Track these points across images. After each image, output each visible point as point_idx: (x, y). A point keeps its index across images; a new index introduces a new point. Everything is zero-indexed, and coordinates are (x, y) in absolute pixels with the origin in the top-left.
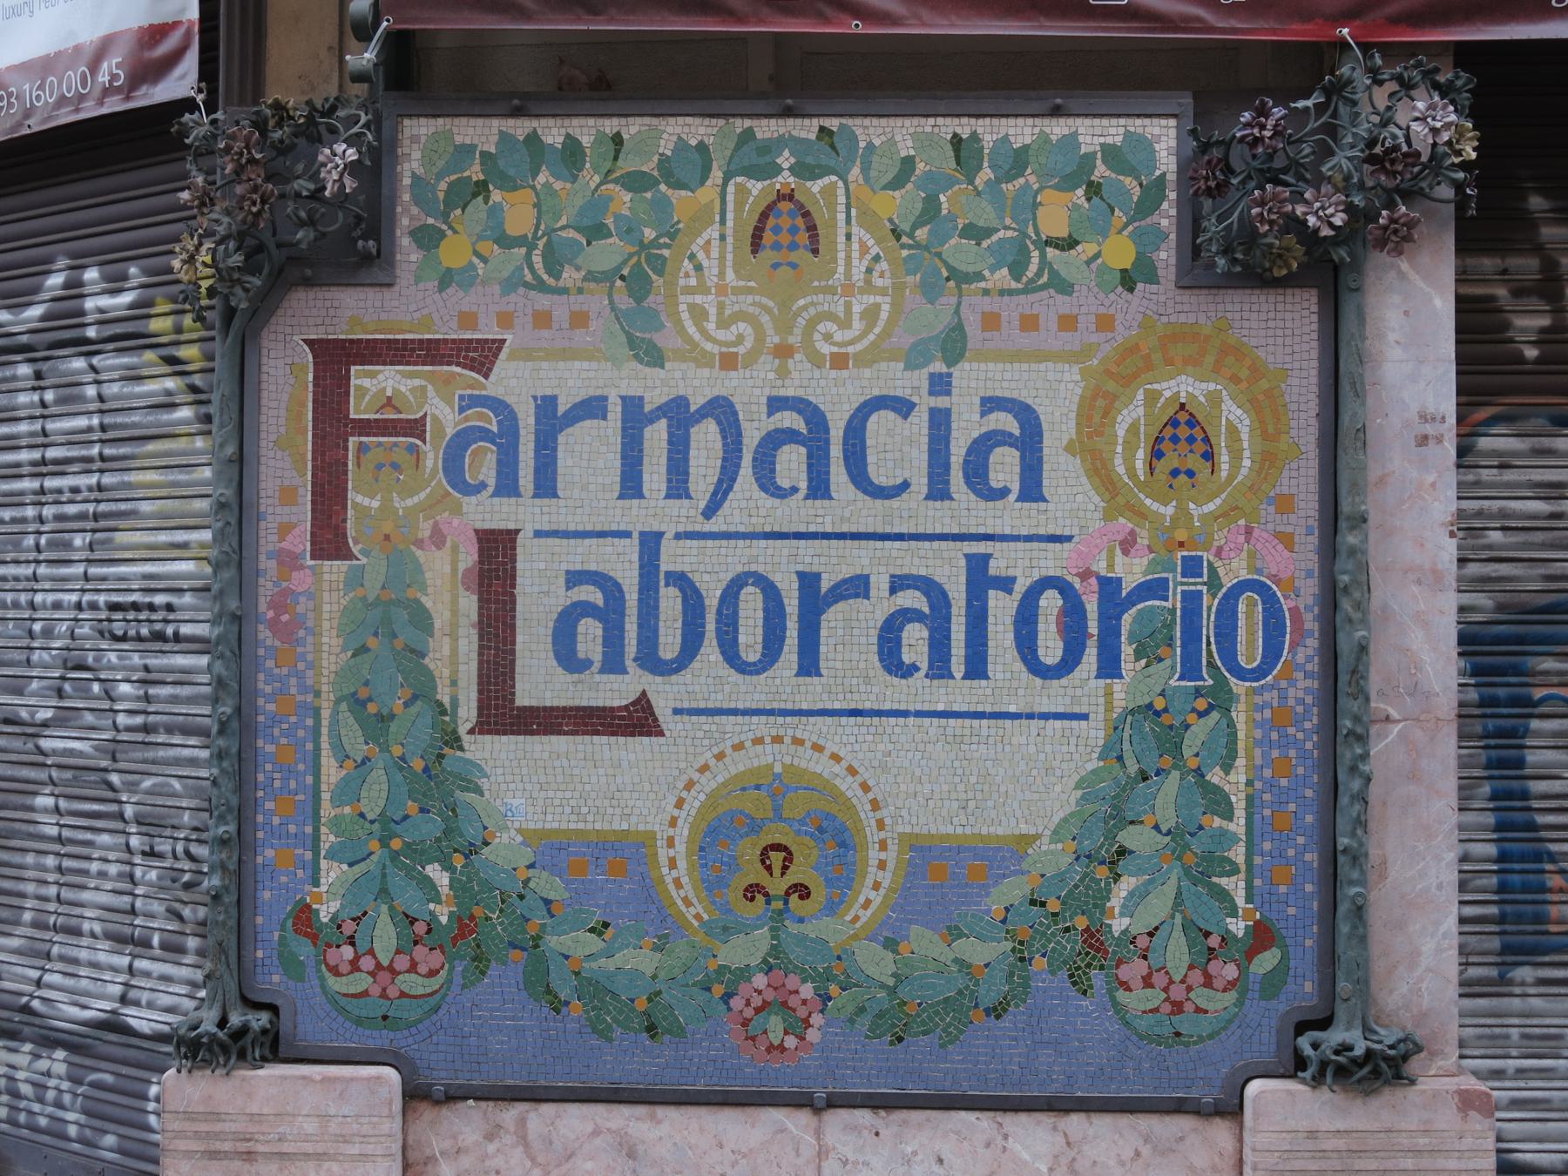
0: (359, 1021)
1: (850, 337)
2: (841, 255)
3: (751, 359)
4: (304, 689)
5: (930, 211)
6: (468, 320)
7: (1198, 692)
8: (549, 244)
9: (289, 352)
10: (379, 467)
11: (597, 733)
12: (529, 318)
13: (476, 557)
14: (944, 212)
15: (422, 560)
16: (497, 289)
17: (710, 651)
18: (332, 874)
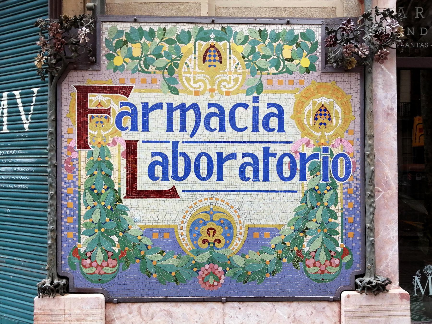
0: (92, 281)
1: (231, 86)
2: (228, 63)
3: (203, 93)
5: (253, 51)
6: (122, 80)
7: (327, 185)
8: (145, 59)
9: (70, 89)
10: (97, 122)
11: (161, 197)
12: (140, 80)
13: (125, 148)
14: (257, 51)
15: (110, 149)
17: (192, 174)
18: (84, 239)
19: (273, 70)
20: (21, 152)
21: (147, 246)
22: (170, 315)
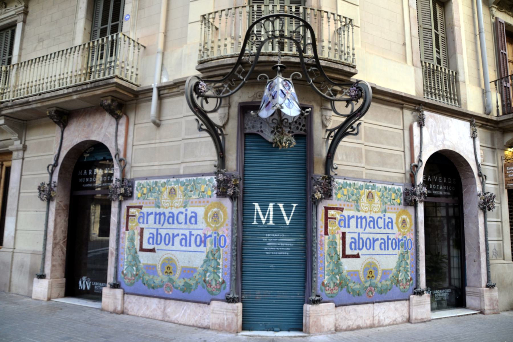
0: (329, 297)
4: (323, 253)
5: (383, 195)
6: (340, 205)
17: (365, 247)
19: (389, 203)
20: (284, 235)
21: (349, 280)
22: (355, 310)
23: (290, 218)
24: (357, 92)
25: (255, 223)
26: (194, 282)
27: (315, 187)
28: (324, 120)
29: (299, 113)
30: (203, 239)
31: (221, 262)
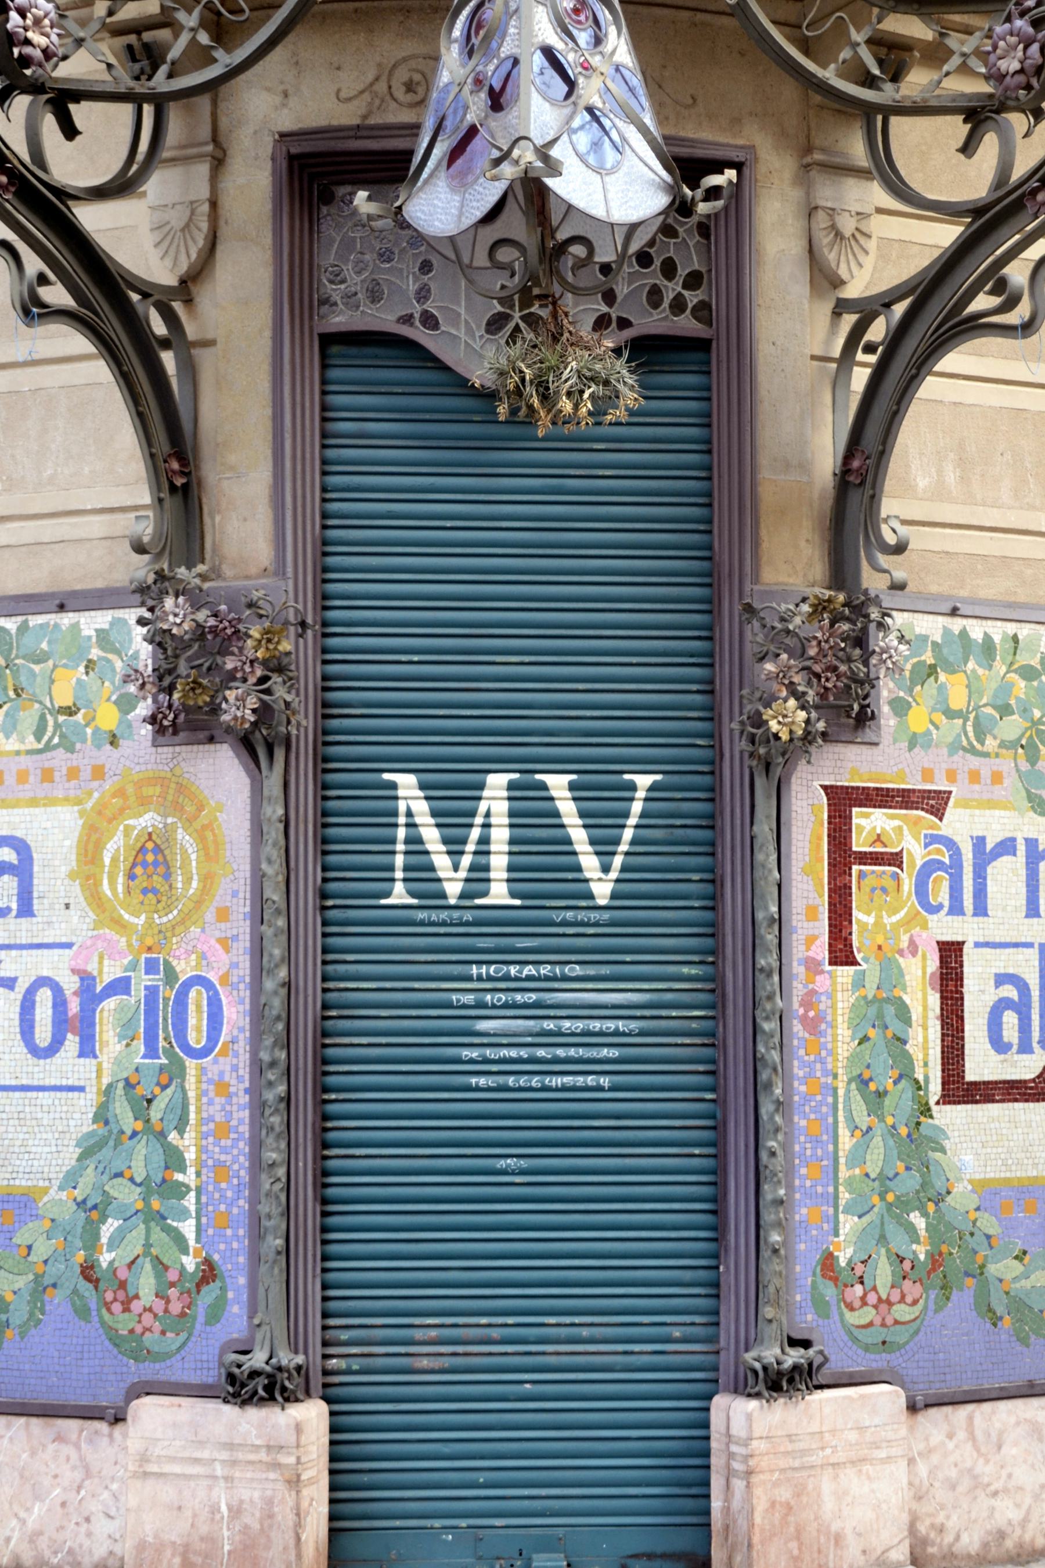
0: (867, 1348)
6: (928, 774)
8: (976, 717)
9: (811, 795)
10: (873, 890)
11: (1016, 1100)
12: (967, 775)
15: (903, 966)
16: (945, 751)
18: (848, 1226)
20: (578, 970)
21: (988, 1237)
23: (618, 861)
24: (1035, 48)
25: (399, 894)
26: (21, 1282)
27: (769, 667)
28: (824, 240)
29: (661, 201)
30: (74, 1006)
31: (188, 1144)
